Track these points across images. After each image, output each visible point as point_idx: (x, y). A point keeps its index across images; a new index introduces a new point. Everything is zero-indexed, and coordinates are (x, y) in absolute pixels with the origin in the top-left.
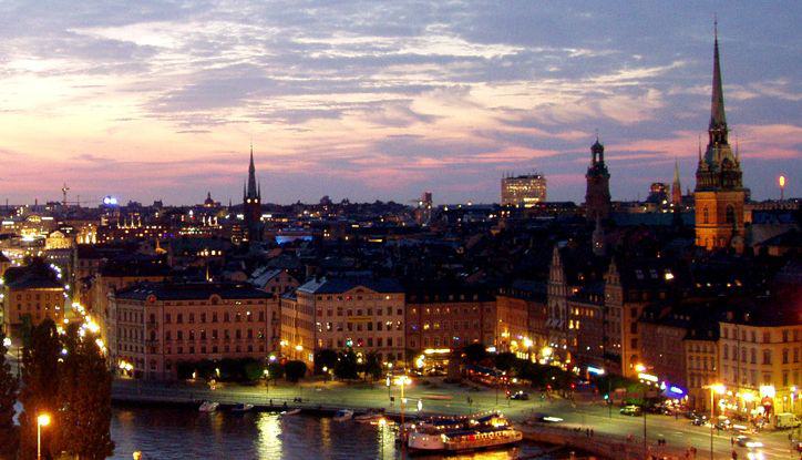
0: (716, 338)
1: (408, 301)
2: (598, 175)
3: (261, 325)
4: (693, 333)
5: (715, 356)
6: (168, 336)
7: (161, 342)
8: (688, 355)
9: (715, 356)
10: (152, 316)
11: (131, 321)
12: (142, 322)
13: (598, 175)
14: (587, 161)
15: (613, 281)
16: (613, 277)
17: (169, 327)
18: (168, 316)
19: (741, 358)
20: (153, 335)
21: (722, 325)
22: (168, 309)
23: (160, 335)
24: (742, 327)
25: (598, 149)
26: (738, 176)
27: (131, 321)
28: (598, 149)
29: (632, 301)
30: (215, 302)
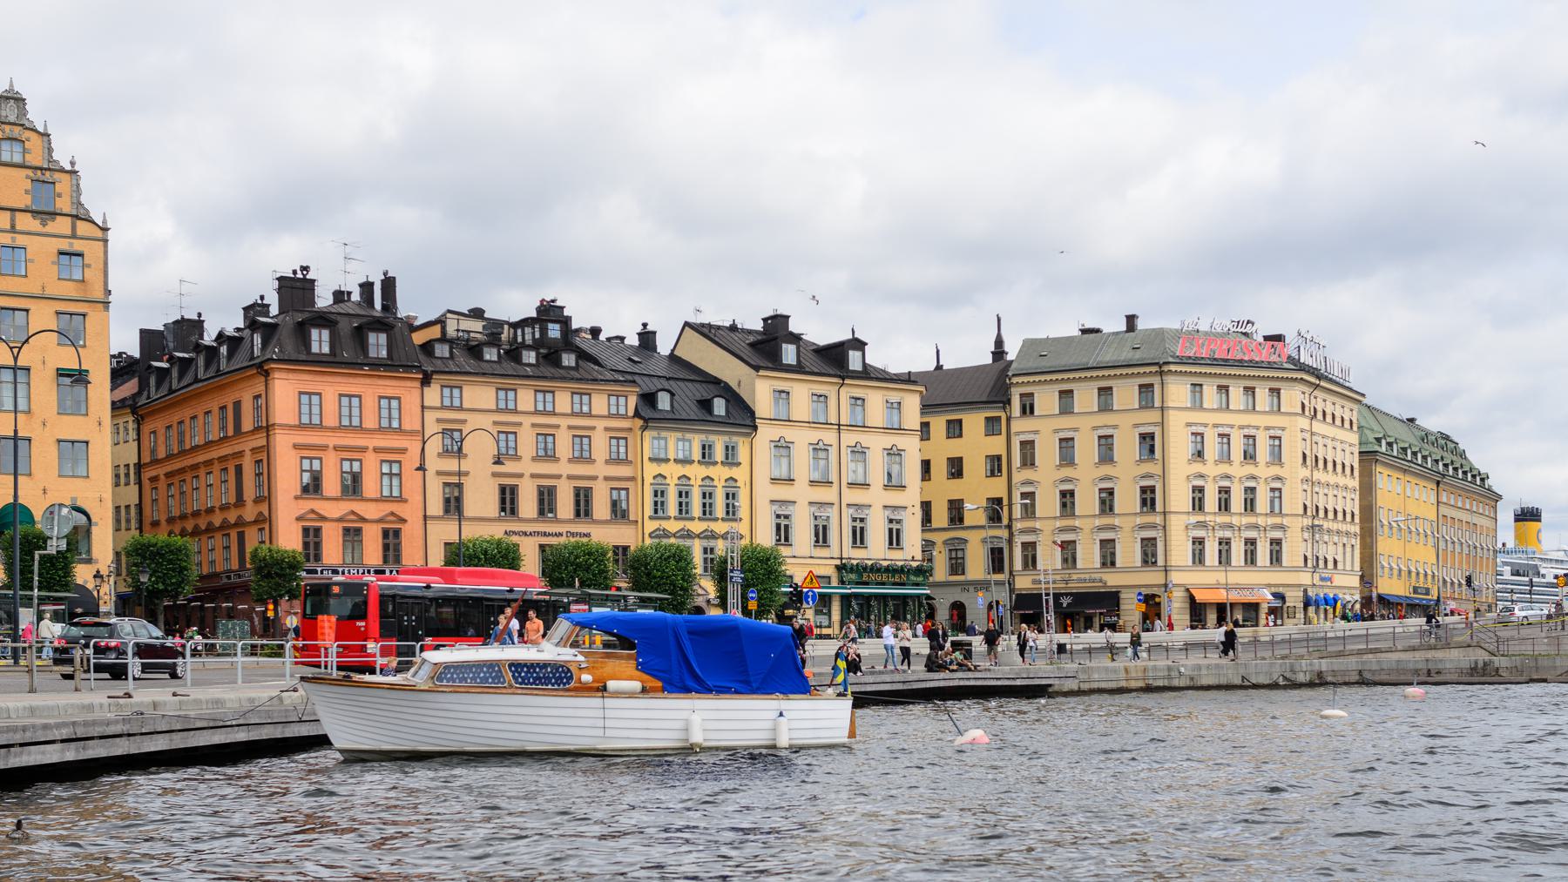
5: (740, 474)
9: (740, 474)
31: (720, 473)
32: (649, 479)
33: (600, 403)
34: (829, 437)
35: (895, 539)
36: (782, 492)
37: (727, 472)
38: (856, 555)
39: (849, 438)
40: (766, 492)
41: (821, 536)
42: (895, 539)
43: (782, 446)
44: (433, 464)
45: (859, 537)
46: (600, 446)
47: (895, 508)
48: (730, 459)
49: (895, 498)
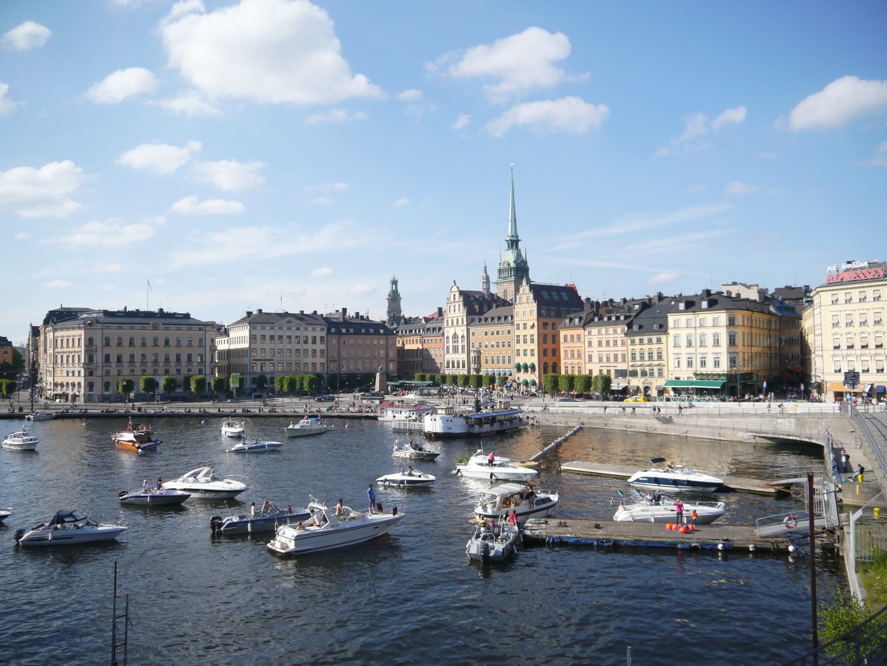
0: (663, 328)
3: (201, 351)
6: (107, 358)
7: (100, 364)
14: (387, 289)
15: (524, 300)
17: (107, 350)
18: (107, 339)
19: (698, 344)
21: (671, 318)
23: (99, 358)
24: (701, 315)
25: (395, 282)
26: (526, 270)
28: (395, 282)
29: (544, 317)
31: (655, 347)
32: (630, 350)
33: (619, 330)
34: (692, 331)
35: (717, 364)
36: (677, 350)
37: (658, 346)
38: (704, 370)
39: (700, 331)
40: (672, 350)
41: (690, 364)
42: (717, 364)
43: (676, 337)
44: (587, 349)
45: (703, 364)
46: (619, 343)
47: (717, 353)
48: (659, 341)
49: (717, 350)
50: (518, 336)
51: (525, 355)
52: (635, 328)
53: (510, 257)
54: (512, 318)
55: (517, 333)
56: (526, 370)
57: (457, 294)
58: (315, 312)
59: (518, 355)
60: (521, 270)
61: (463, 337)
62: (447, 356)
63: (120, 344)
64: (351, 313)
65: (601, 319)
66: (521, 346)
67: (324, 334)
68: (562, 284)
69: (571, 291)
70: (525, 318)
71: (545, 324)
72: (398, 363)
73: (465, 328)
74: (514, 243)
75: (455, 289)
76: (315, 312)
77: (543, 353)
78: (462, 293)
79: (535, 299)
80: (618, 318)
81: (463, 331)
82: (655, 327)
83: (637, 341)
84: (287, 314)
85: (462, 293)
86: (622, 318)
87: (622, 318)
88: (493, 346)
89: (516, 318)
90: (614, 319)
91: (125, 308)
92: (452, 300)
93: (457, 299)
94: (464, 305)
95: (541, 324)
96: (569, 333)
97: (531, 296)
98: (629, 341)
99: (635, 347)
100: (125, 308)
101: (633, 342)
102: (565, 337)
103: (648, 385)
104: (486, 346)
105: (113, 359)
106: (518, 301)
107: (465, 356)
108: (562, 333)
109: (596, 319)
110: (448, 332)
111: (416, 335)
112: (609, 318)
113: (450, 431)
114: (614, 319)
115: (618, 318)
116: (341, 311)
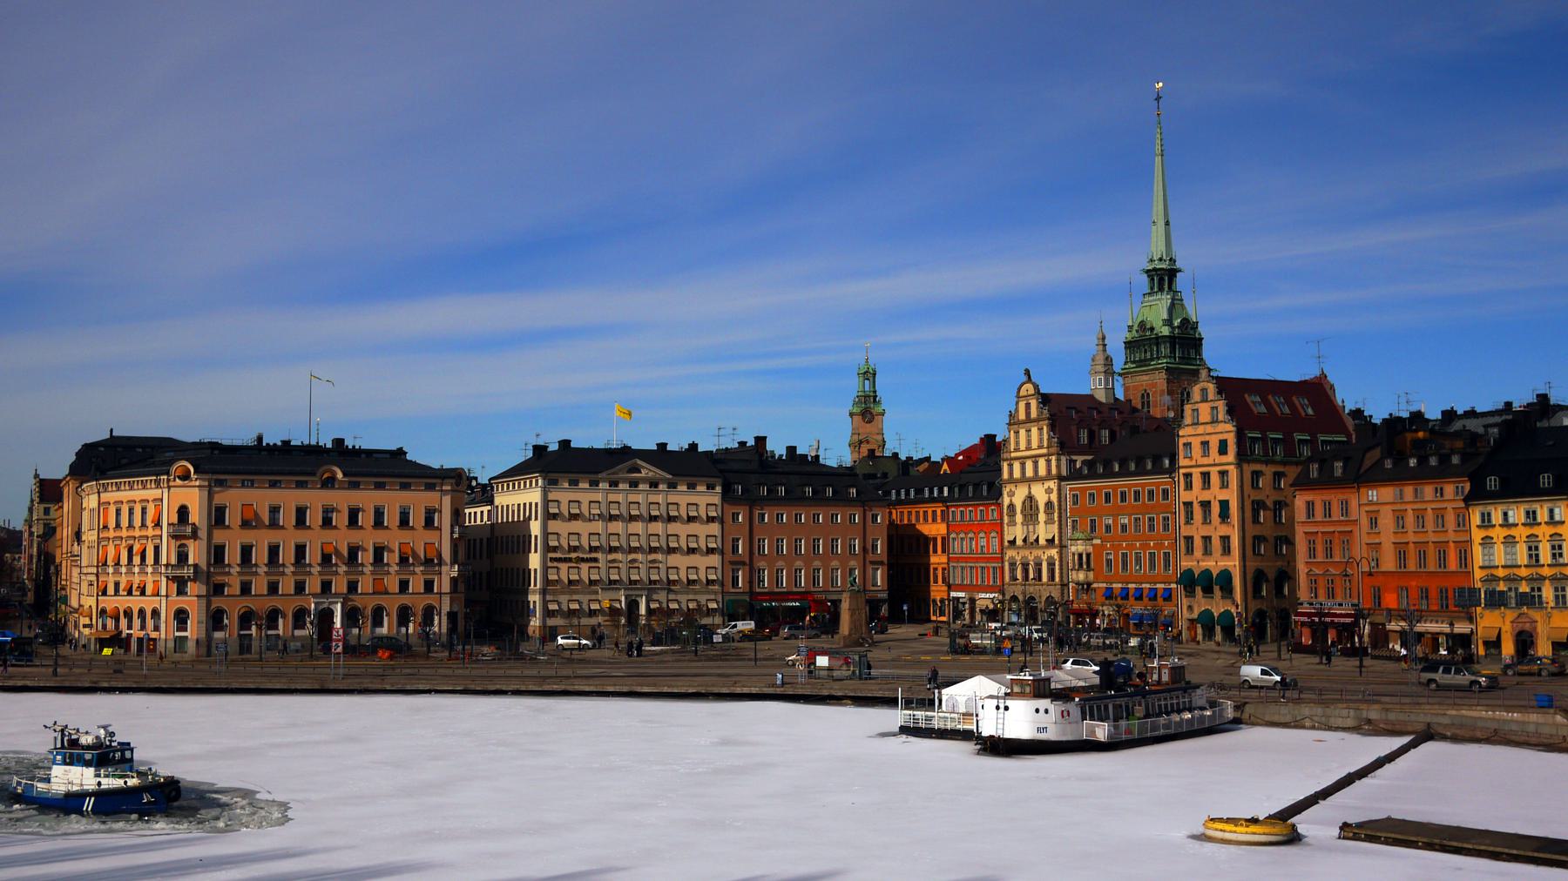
1: (727, 495)
2: (867, 409)
4: (1492, 483)
8: (1477, 535)
10: (183, 512)
11: (131, 526)
12: (158, 524)
13: (867, 409)
15: (1205, 416)
16: (1204, 409)
20: (182, 557)
22: (225, 497)
25: (869, 375)
26: (1197, 343)
27: (131, 526)
30: (329, 483)
33: (1449, 490)
50: (1188, 505)
51: (1207, 552)
52: (1492, 483)
53: (1156, 312)
54: (1173, 458)
55: (1186, 496)
56: (1208, 591)
57: (1034, 403)
58: (693, 446)
59: (1190, 550)
60: (1185, 341)
61: (1049, 504)
62: (1010, 553)
63: (379, 523)
64: (776, 447)
65: (1400, 459)
66: (1197, 530)
67: (717, 500)
68: (1294, 376)
69: (1317, 390)
70: (1206, 461)
71: (1256, 475)
72: (890, 566)
73: (1052, 484)
74: (1163, 277)
75: (1029, 388)
76: (693, 446)
77: (1253, 544)
78: (1045, 399)
79: (1229, 412)
80: (1444, 459)
81: (1049, 491)
82: (1545, 480)
83: (1497, 518)
84: (625, 453)
85: (1045, 399)
86: (1455, 460)
87: (1455, 460)
88: (1124, 527)
89: (1183, 462)
90: (1433, 461)
91: (260, 439)
92: (1022, 416)
93: (1034, 414)
94: (1052, 427)
95: (1247, 477)
96: (1318, 498)
97: (1222, 406)
98: (1476, 519)
99: (1535, 530)
100: (260, 439)
101: (1486, 522)
102: (1310, 506)
103: (1527, 627)
104: (1108, 527)
105: (233, 556)
106: (1188, 420)
107: (1054, 552)
108: (1300, 501)
109: (1388, 464)
110: (1011, 494)
111: (932, 500)
112: (1423, 460)
113: (1043, 736)
114: (1433, 461)
115: (1444, 459)
116: (751, 442)
